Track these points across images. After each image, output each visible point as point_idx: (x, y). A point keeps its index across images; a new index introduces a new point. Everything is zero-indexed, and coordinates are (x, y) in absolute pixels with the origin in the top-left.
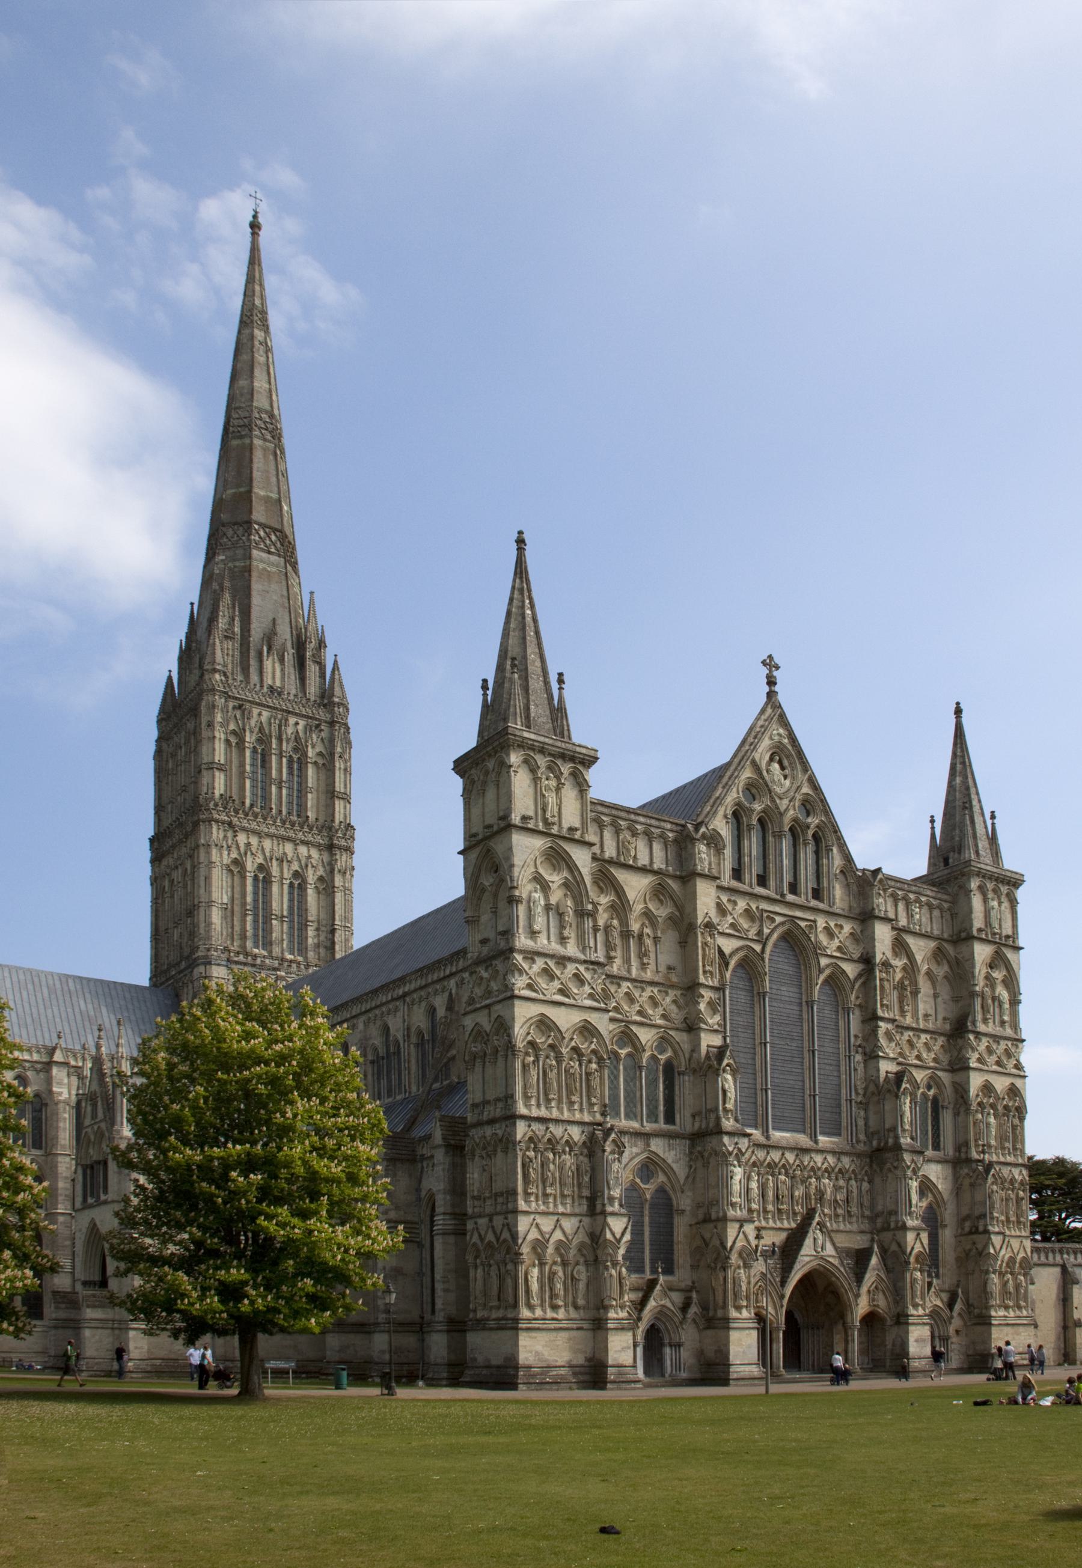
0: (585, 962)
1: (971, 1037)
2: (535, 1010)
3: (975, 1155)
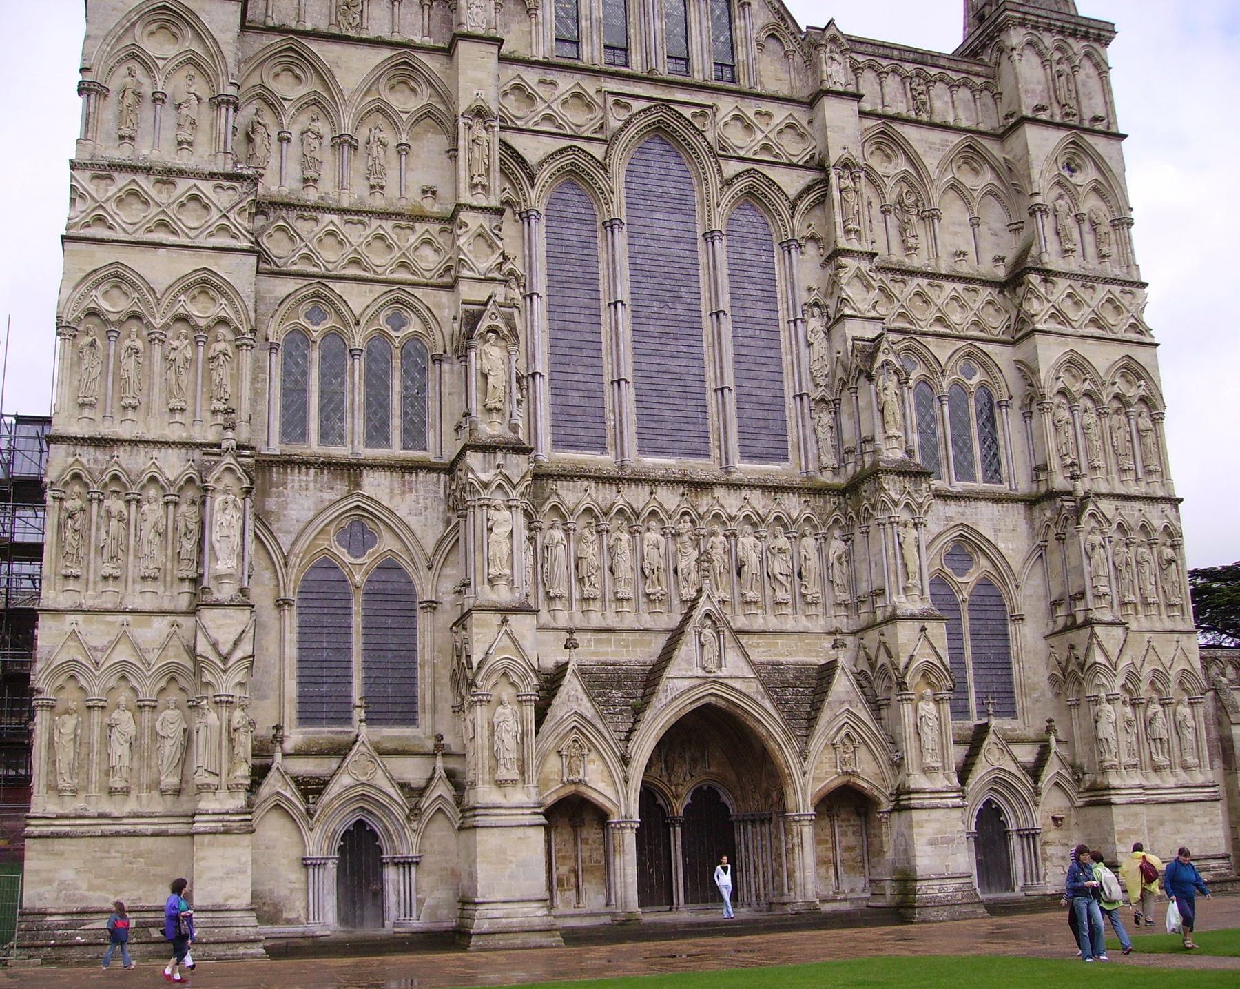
0: (212, 175)
1: (1034, 279)
2: (103, 257)
3: (1059, 481)
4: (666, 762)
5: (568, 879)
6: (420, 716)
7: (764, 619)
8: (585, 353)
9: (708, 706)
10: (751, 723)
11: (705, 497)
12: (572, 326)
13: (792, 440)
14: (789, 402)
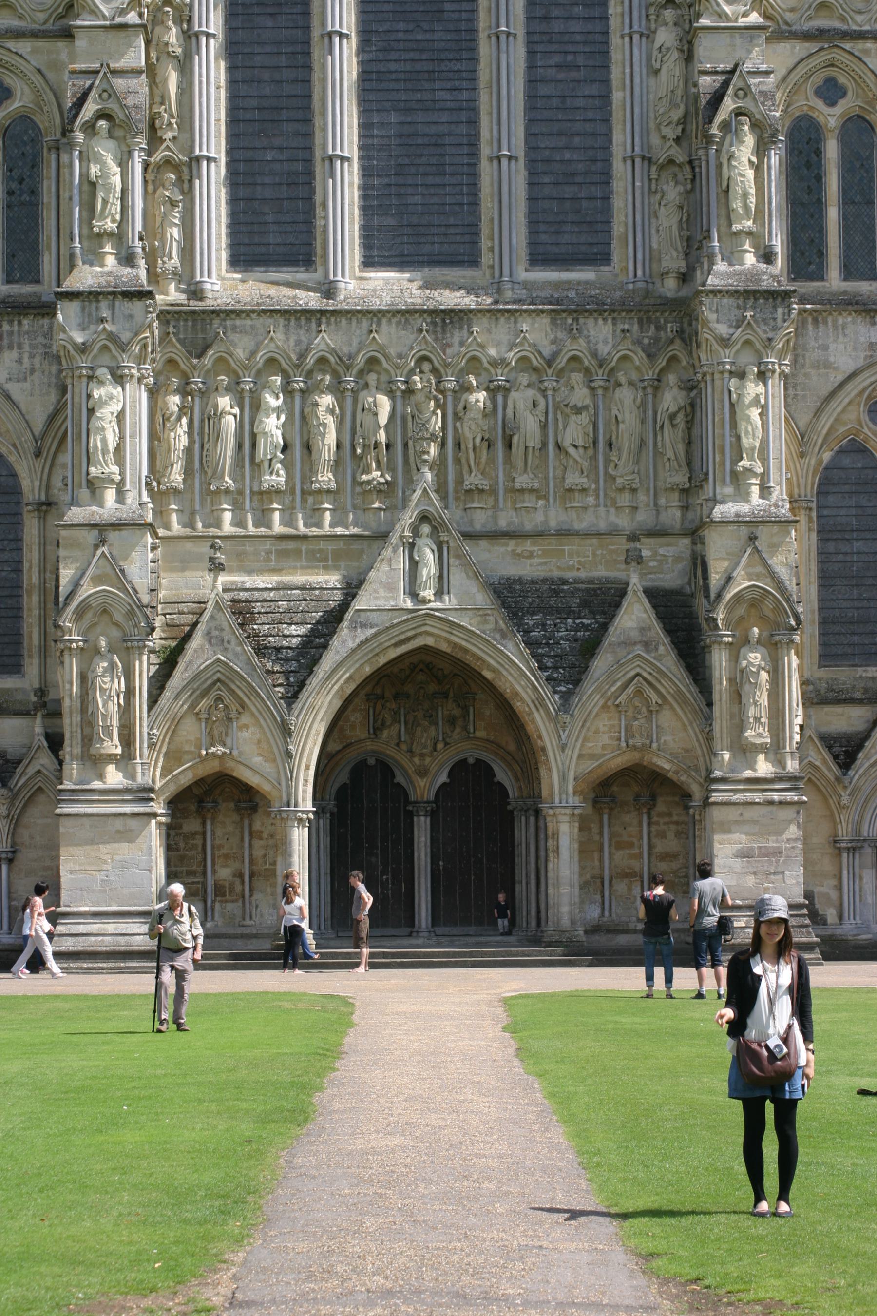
4: (406, 723)
5: (232, 885)
6: (26, 661)
7: (546, 516)
8: (284, 114)
9: (425, 649)
10: (488, 675)
11: (457, 333)
12: (266, 75)
13: (617, 229)
14: (620, 169)
